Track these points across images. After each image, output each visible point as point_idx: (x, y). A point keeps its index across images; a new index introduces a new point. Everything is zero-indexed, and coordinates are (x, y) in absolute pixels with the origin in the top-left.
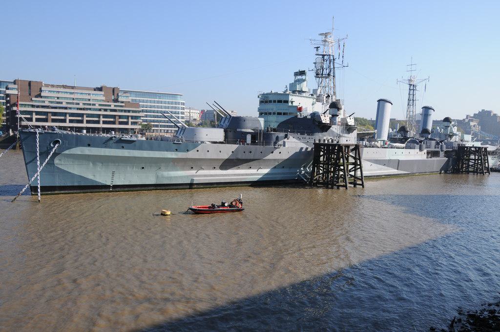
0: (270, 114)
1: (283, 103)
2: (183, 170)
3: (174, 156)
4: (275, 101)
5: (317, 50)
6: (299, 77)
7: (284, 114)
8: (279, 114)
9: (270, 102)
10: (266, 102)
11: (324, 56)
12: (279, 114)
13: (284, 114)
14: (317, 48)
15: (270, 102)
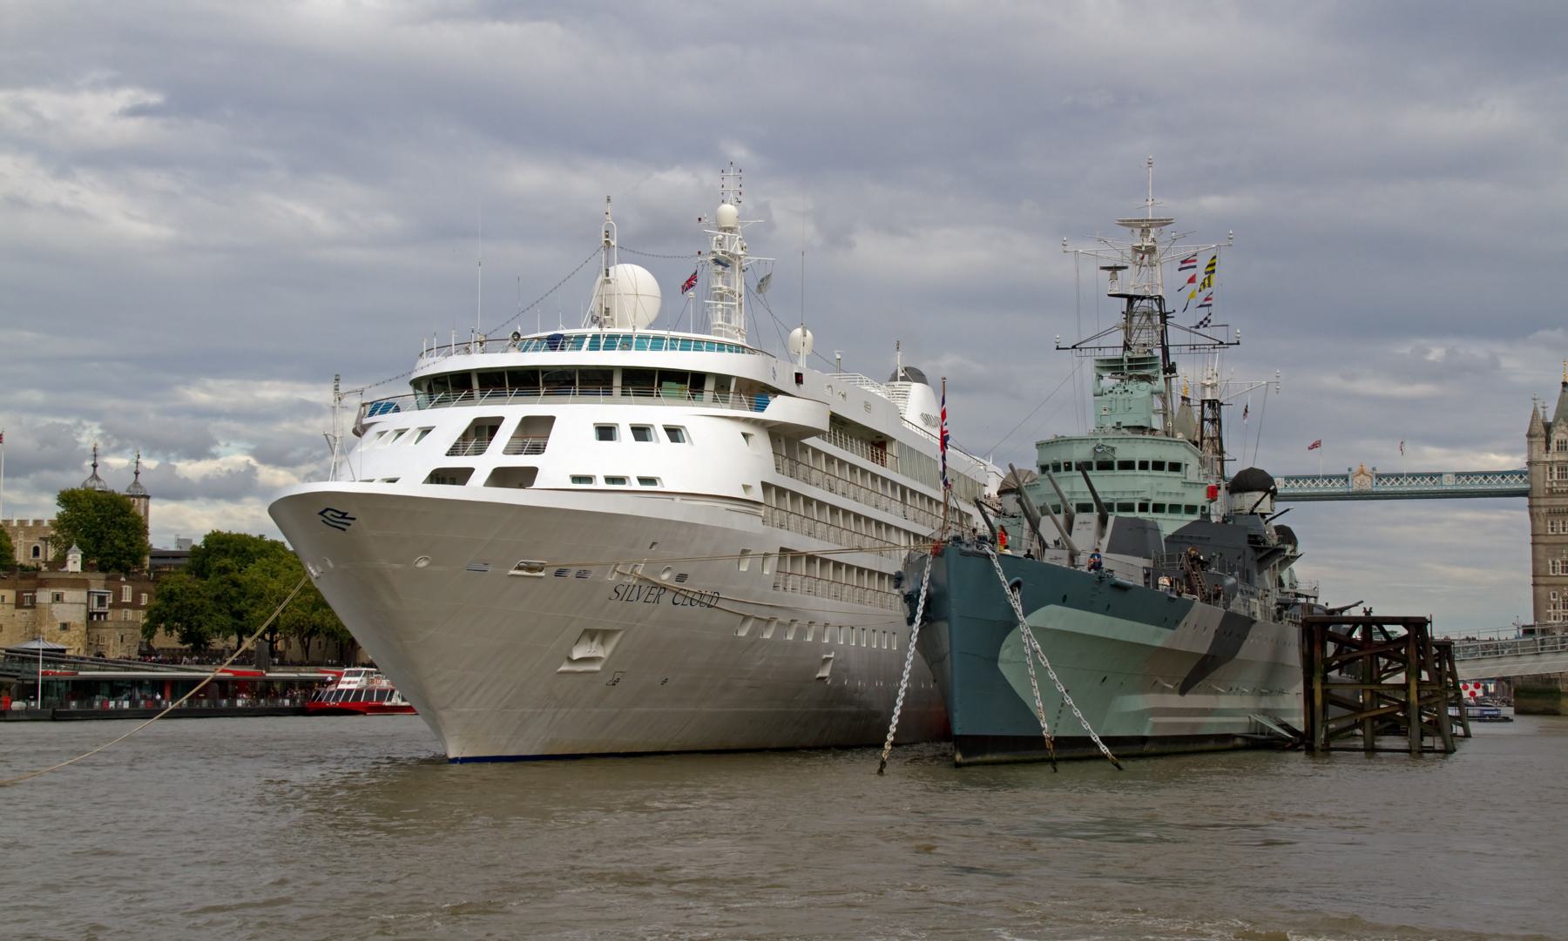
0: (1127, 507)
1: (1166, 473)
2: (1143, 691)
3: (1158, 643)
4: (1144, 465)
5: (1114, 278)
6: (1109, 381)
7: (1175, 508)
8: (1158, 508)
9: (1127, 465)
10: (1105, 466)
11: (1131, 299)
12: (1158, 508)
13: (1175, 508)
14: (1115, 269)
15: (1127, 465)
